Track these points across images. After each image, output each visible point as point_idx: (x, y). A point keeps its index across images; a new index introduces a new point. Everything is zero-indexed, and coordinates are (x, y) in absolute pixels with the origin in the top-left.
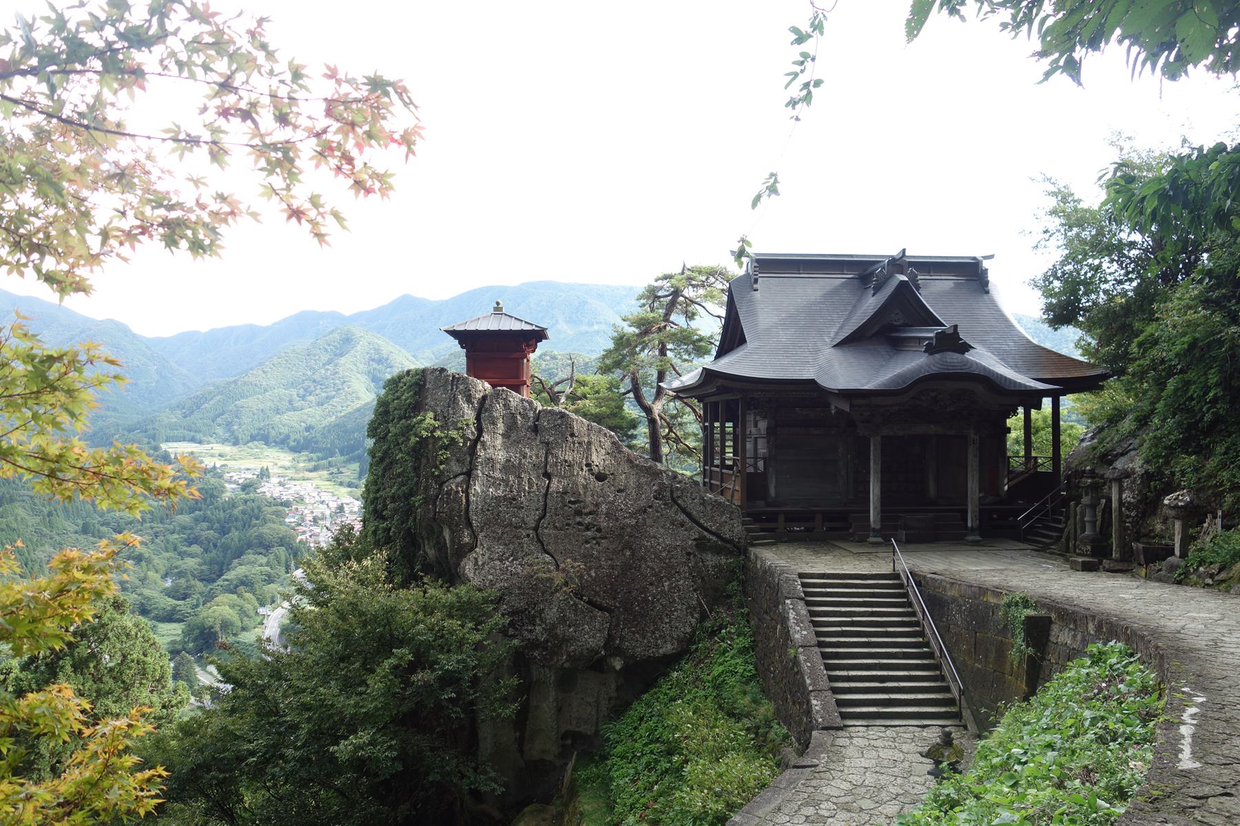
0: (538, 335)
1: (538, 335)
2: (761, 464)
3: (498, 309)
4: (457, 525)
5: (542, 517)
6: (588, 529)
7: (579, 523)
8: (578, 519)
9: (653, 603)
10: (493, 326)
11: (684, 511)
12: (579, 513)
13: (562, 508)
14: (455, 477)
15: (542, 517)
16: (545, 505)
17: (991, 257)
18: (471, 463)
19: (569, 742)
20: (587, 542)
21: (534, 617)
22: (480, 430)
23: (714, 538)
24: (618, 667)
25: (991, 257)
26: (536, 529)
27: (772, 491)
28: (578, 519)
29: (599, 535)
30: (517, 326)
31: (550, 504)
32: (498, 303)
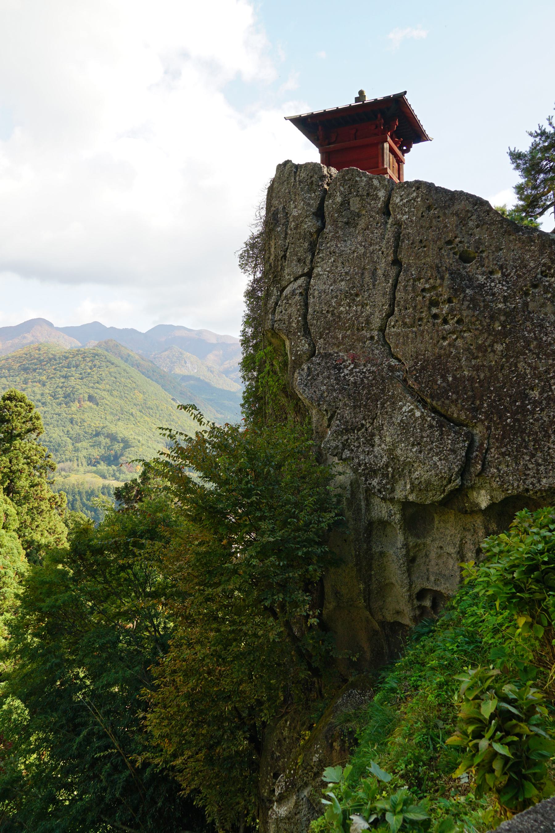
4: (295, 334)
5: (391, 313)
6: (445, 322)
7: (435, 316)
13: (414, 299)
14: (296, 279)
15: (391, 313)
18: (312, 261)
19: (428, 603)
20: (444, 339)
21: (373, 435)
24: (484, 505)
26: (382, 330)
28: (434, 311)
29: (460, 327)
31: (398, 295)
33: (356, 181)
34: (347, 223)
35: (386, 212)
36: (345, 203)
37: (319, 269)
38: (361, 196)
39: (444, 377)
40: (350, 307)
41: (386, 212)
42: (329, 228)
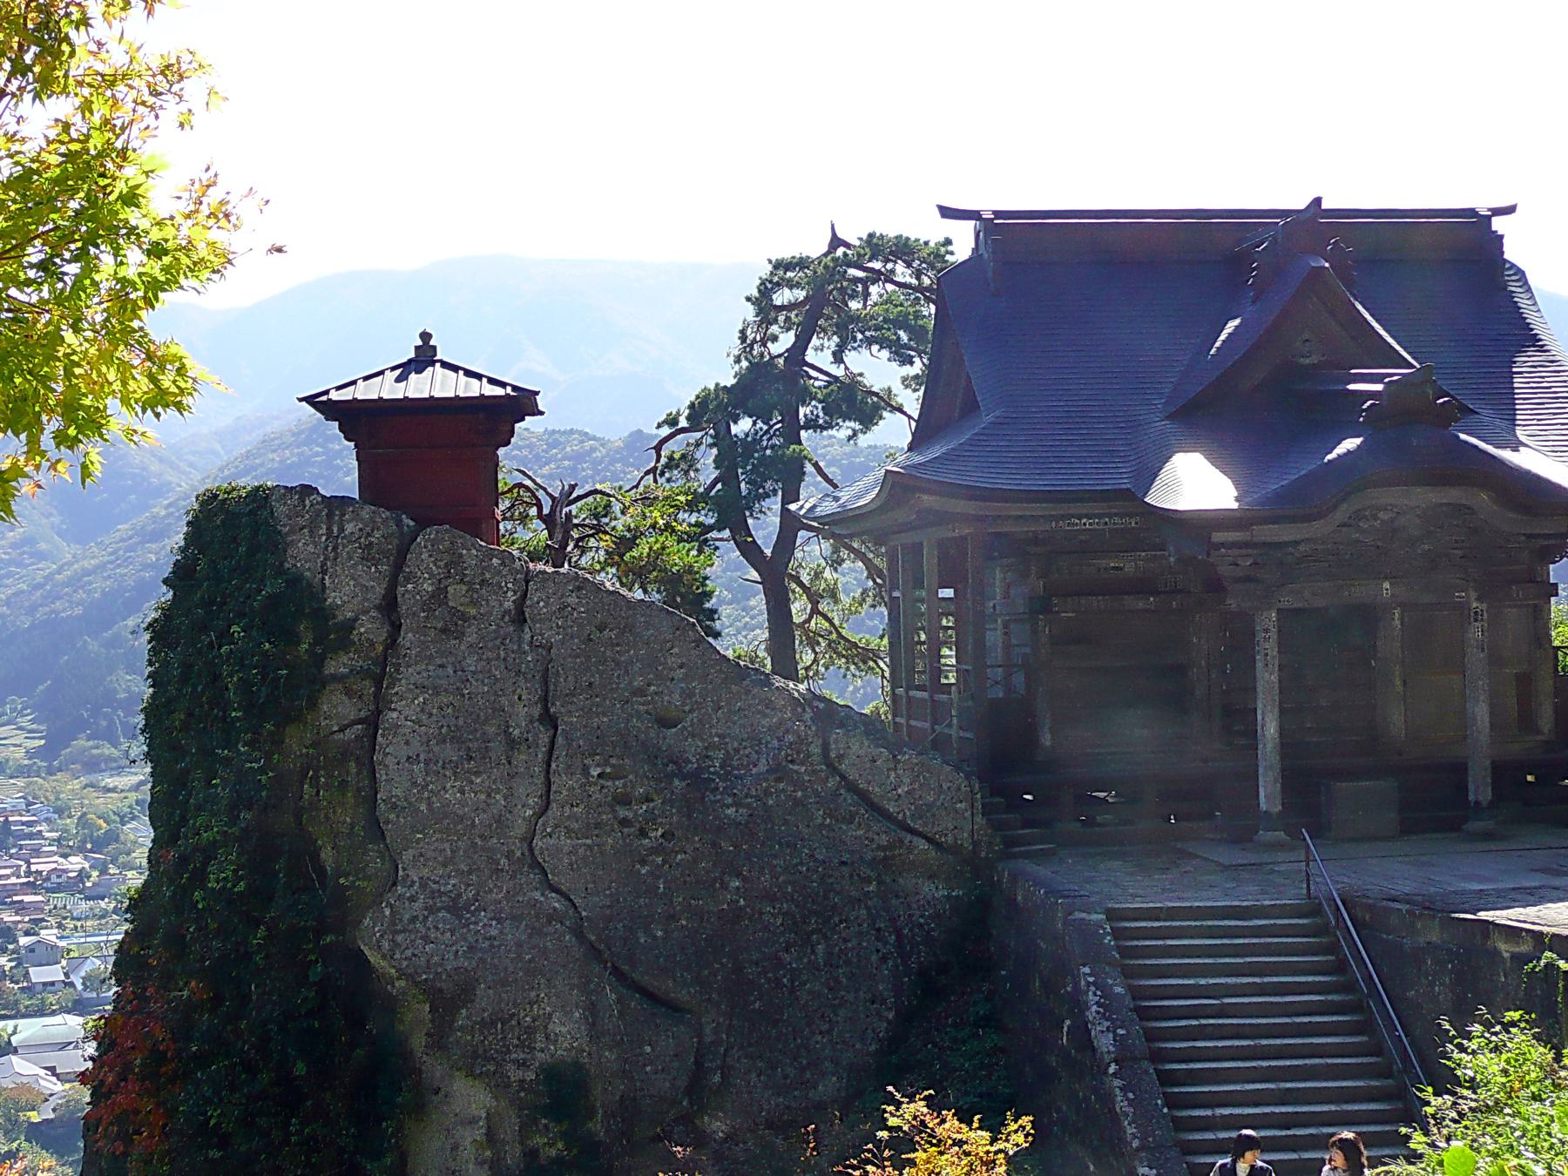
0: (522, 403)
1: (522, 403)
2: (1019, 679)
3: (424, 357)
6: (643, 833)
7: (624, 822)
8: (622, 812)
9: (792, 991)
10: (420, 387)
11: (852, 788)
12: (624, 800)
16: (548, 784)
17: (1510, 210)
18: (377, 695)
20: (643, 862)
21: (530, 1031)
22: (396, 627)
23: (922, 844)
25: (1510, 210)
27: (1047, 739)
28: (622, 812)
30: (474, 389)
32: (426, 336)
33: (461, 555)
34: (444, 631)
35: (520, 618)
36: (440, 595)
37: (395, 715)
38: (470, 583)
39: (647, 931)
40: (463, 793)
41: (520, 618)
42: (407, 638)
